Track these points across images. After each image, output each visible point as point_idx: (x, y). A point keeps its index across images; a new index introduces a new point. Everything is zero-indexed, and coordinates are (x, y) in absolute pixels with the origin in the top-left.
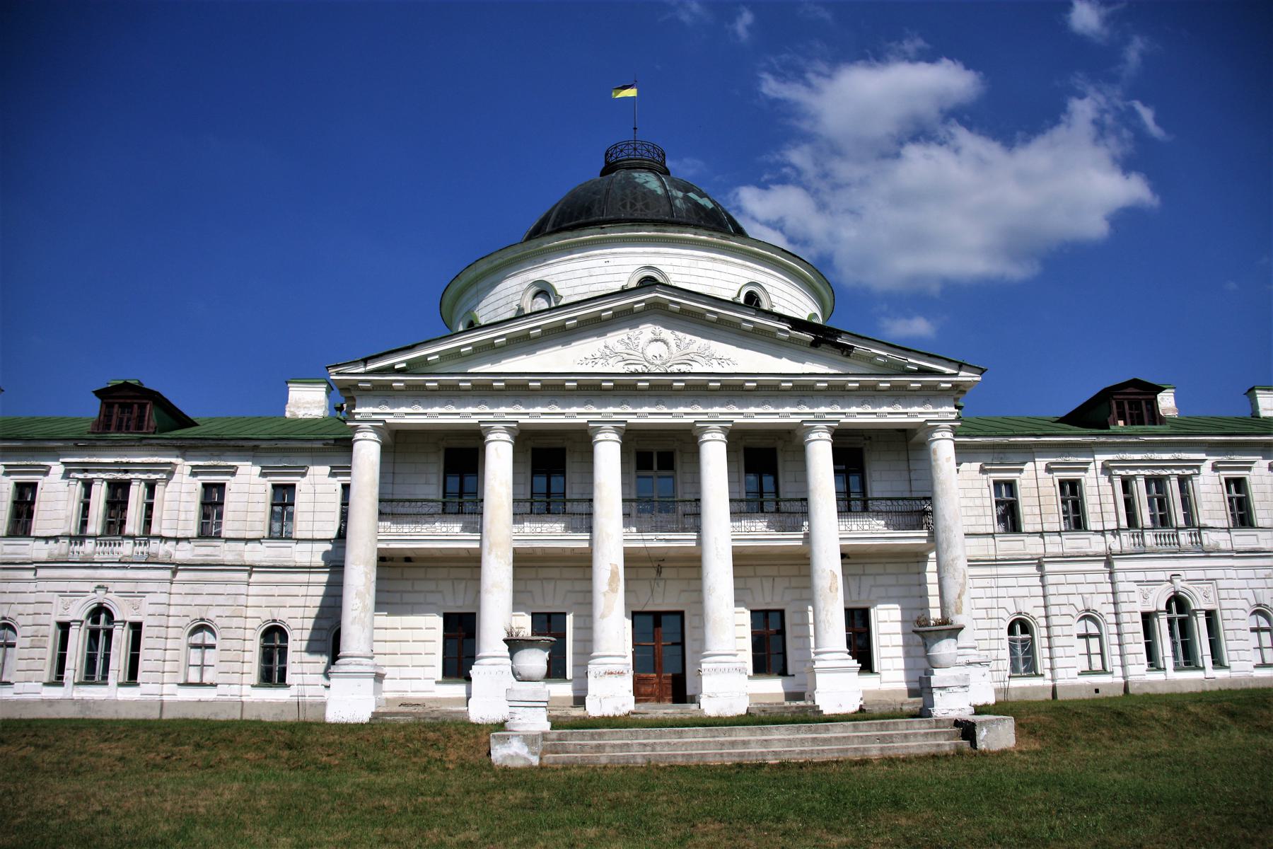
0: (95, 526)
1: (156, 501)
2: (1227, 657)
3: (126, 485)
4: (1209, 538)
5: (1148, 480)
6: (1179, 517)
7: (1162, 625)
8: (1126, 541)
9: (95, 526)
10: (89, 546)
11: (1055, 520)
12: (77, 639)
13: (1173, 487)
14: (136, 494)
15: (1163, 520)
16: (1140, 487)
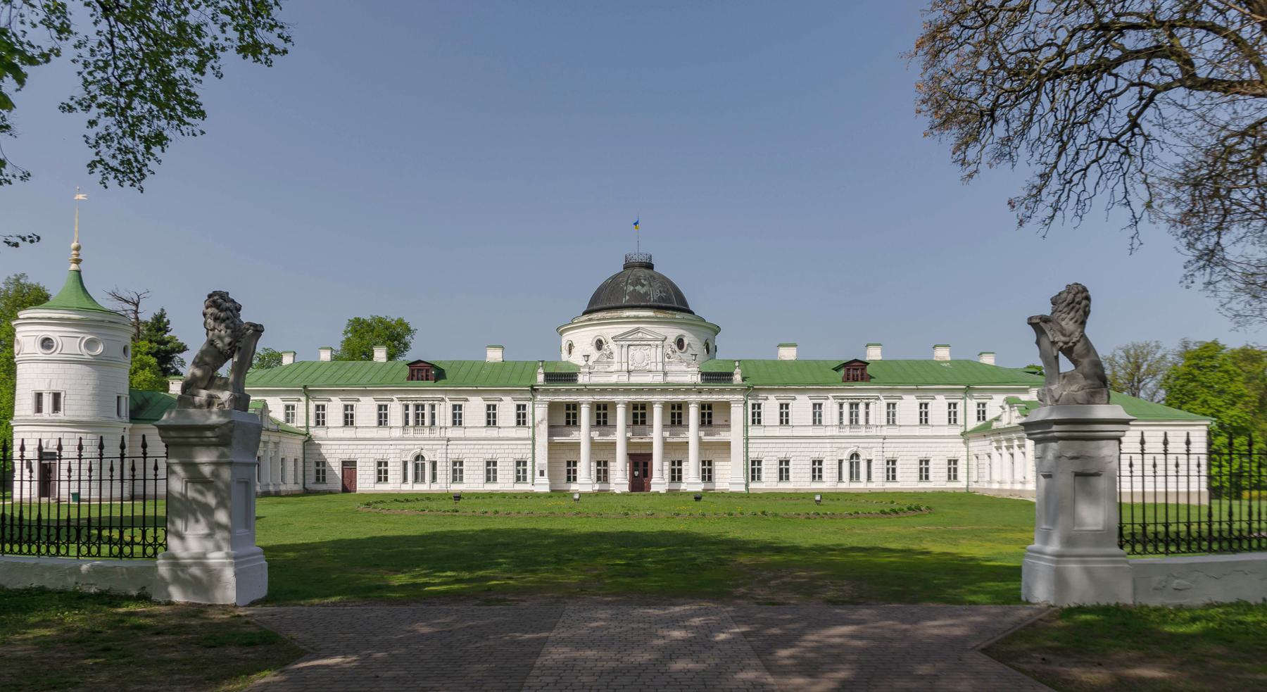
0: (411, 422)
1: (436, 412)
2: (873, 478)
3: (423, 406)
4: (873, 432)
5: (851, 405)
6: (862, 420)
7: (846, 466)
8: (835, 432)
9: (411, 422)
10: (411, 433)
12: (410, 467)
13: (862, 407)
14: (427, 408)
15: (854, 421)
16: (846, 407)
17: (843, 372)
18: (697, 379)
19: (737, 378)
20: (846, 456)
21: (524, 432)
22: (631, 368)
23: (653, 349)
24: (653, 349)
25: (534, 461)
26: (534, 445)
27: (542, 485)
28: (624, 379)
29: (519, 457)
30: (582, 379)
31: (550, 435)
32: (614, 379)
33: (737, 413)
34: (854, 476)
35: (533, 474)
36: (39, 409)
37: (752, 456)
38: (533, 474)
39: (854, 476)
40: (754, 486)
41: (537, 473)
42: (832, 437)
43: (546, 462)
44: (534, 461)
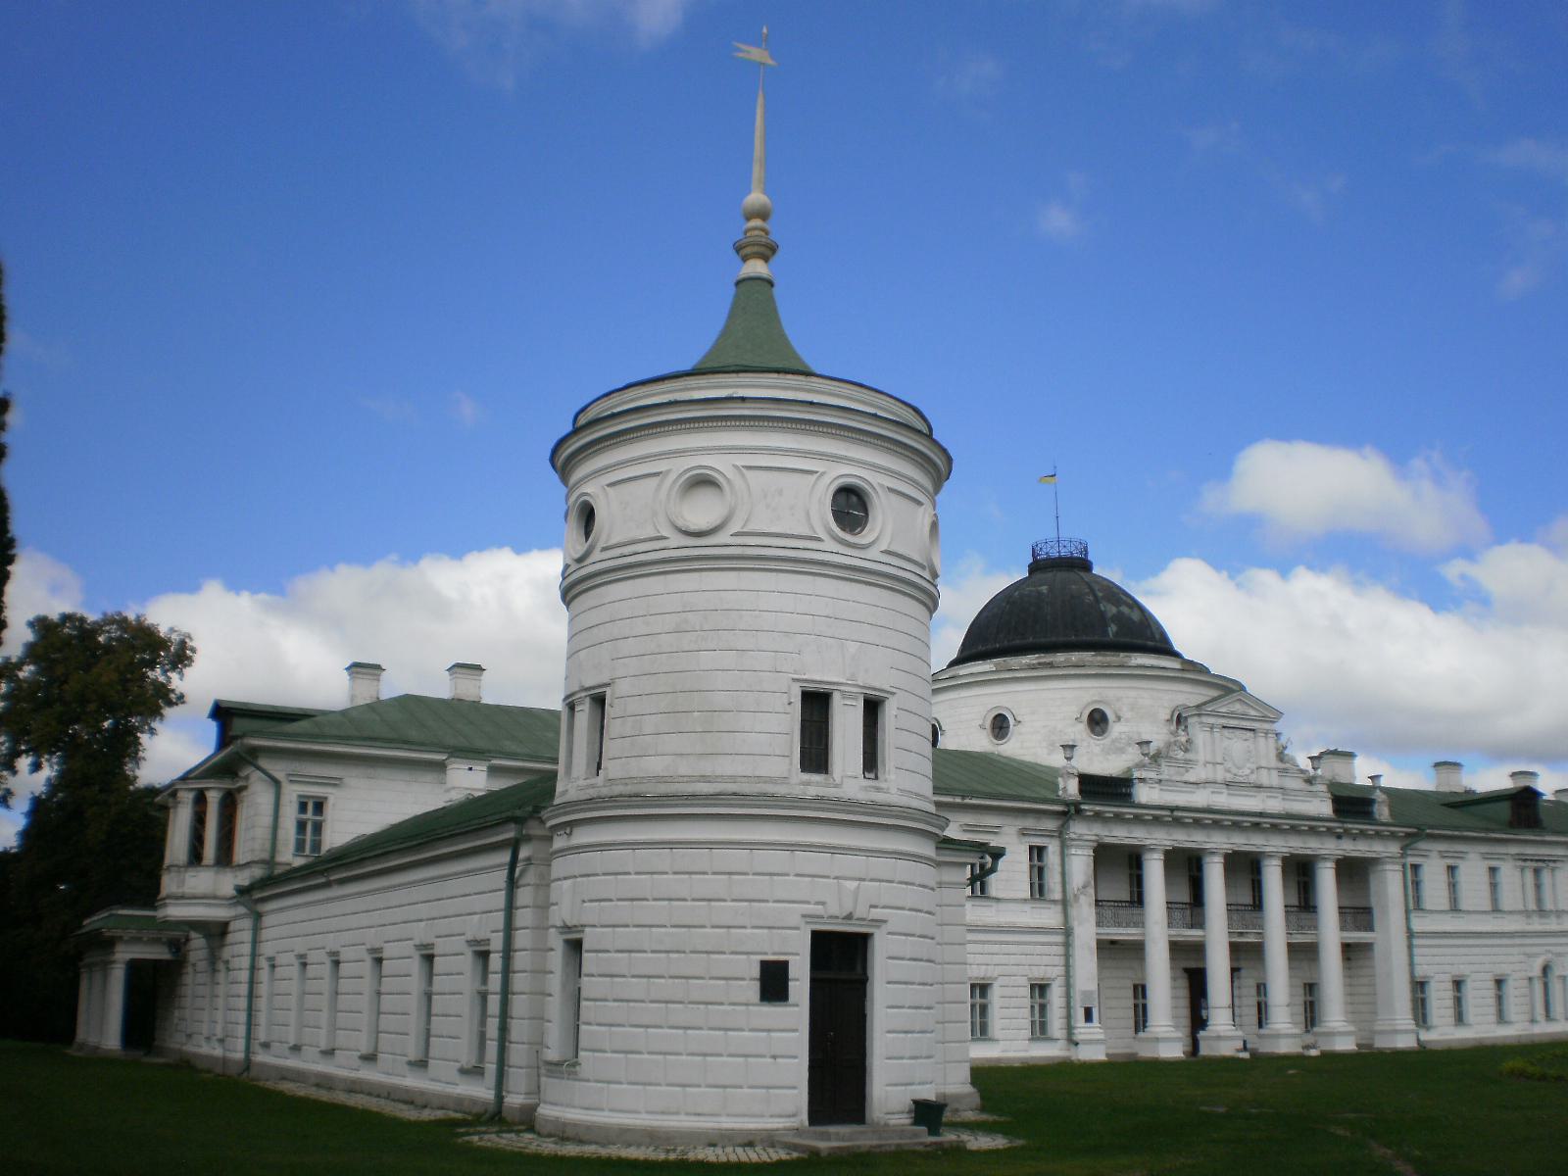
11: (1445, 905)
17: (1504, 810)
18: (1325, 808)
19: (1382, 812)
20: (1537, 972)
21: (1050, 916)
22: (1229, 777)
23: (1261, 741)
24: (1261, 741)
25: (1068, 986)
26: (1067, 945)
27: (1095, 1045)
28: (1223, 800)
29: (1038, 973)
30: (1144, 794)
31: (1098, 924)
32: (1200, 798)
33: (1390, 885)
34: (1548, 1015)
35: (1069, 1017)
36: (815, 754)
37: (1420, 972)
38: (1069, 1017)
39: (1548, 1015)
40: (1425, 1036)
41: (1080, 1014)
42: (1523, 934)
43: (1093, 986)
44: (1068, 986)
